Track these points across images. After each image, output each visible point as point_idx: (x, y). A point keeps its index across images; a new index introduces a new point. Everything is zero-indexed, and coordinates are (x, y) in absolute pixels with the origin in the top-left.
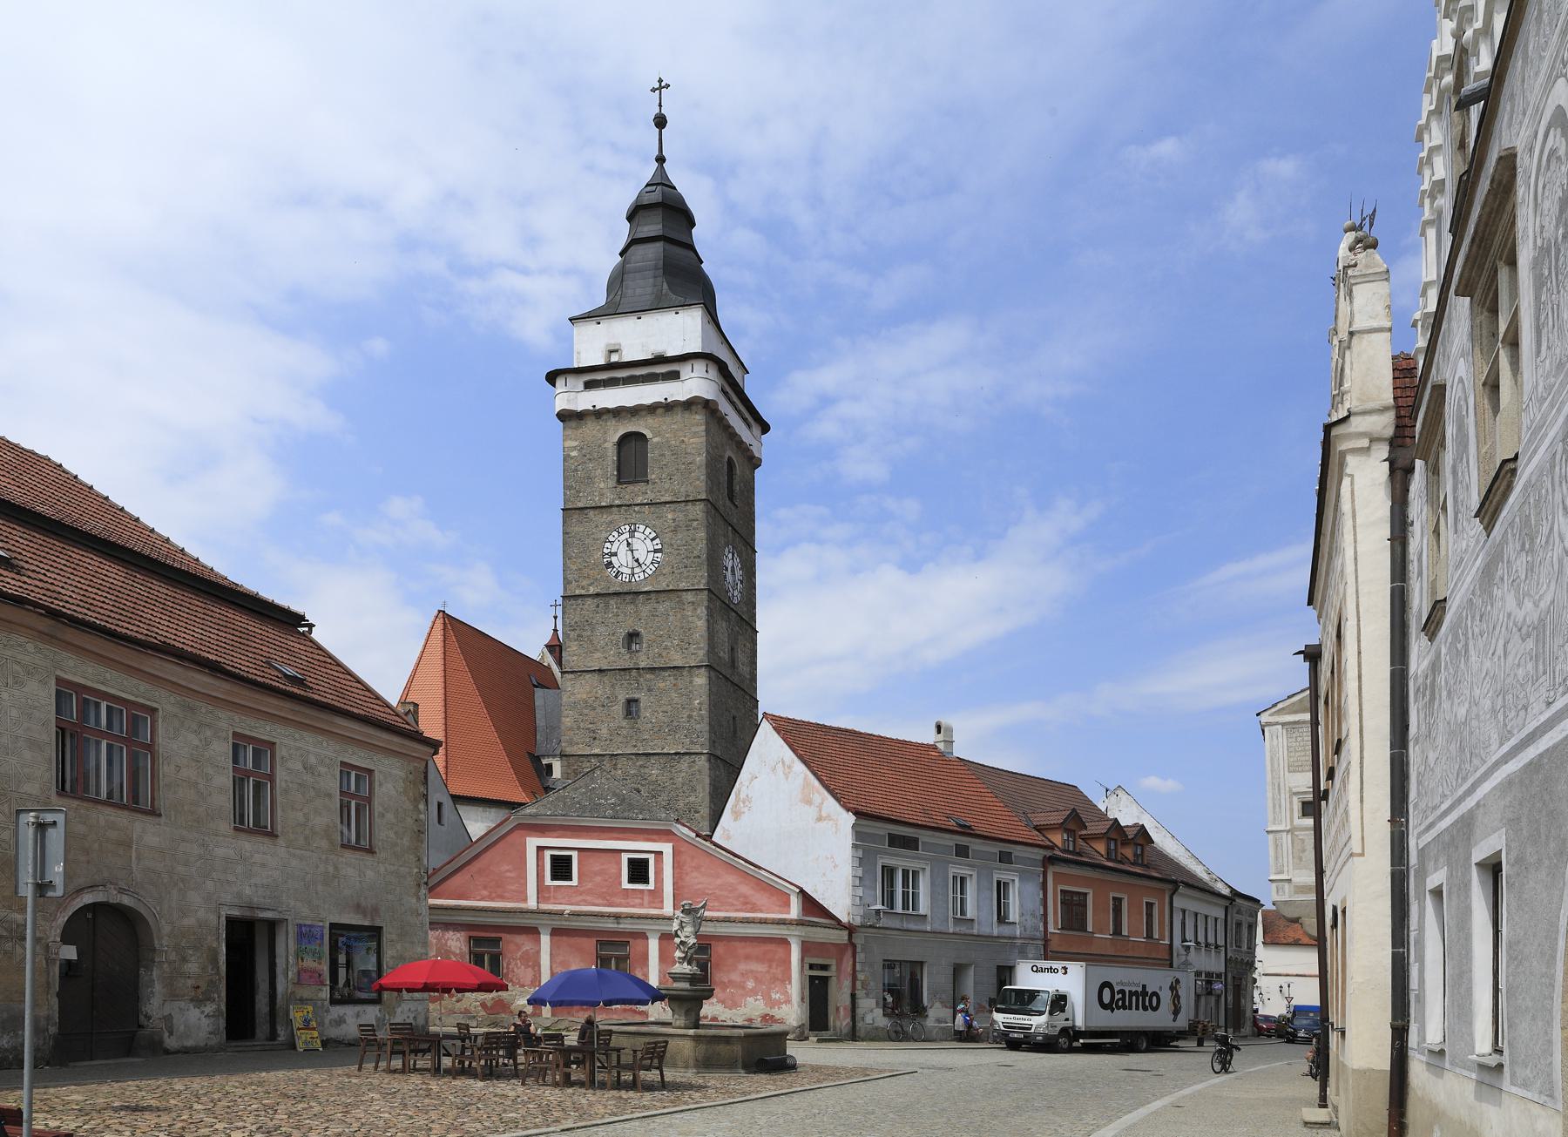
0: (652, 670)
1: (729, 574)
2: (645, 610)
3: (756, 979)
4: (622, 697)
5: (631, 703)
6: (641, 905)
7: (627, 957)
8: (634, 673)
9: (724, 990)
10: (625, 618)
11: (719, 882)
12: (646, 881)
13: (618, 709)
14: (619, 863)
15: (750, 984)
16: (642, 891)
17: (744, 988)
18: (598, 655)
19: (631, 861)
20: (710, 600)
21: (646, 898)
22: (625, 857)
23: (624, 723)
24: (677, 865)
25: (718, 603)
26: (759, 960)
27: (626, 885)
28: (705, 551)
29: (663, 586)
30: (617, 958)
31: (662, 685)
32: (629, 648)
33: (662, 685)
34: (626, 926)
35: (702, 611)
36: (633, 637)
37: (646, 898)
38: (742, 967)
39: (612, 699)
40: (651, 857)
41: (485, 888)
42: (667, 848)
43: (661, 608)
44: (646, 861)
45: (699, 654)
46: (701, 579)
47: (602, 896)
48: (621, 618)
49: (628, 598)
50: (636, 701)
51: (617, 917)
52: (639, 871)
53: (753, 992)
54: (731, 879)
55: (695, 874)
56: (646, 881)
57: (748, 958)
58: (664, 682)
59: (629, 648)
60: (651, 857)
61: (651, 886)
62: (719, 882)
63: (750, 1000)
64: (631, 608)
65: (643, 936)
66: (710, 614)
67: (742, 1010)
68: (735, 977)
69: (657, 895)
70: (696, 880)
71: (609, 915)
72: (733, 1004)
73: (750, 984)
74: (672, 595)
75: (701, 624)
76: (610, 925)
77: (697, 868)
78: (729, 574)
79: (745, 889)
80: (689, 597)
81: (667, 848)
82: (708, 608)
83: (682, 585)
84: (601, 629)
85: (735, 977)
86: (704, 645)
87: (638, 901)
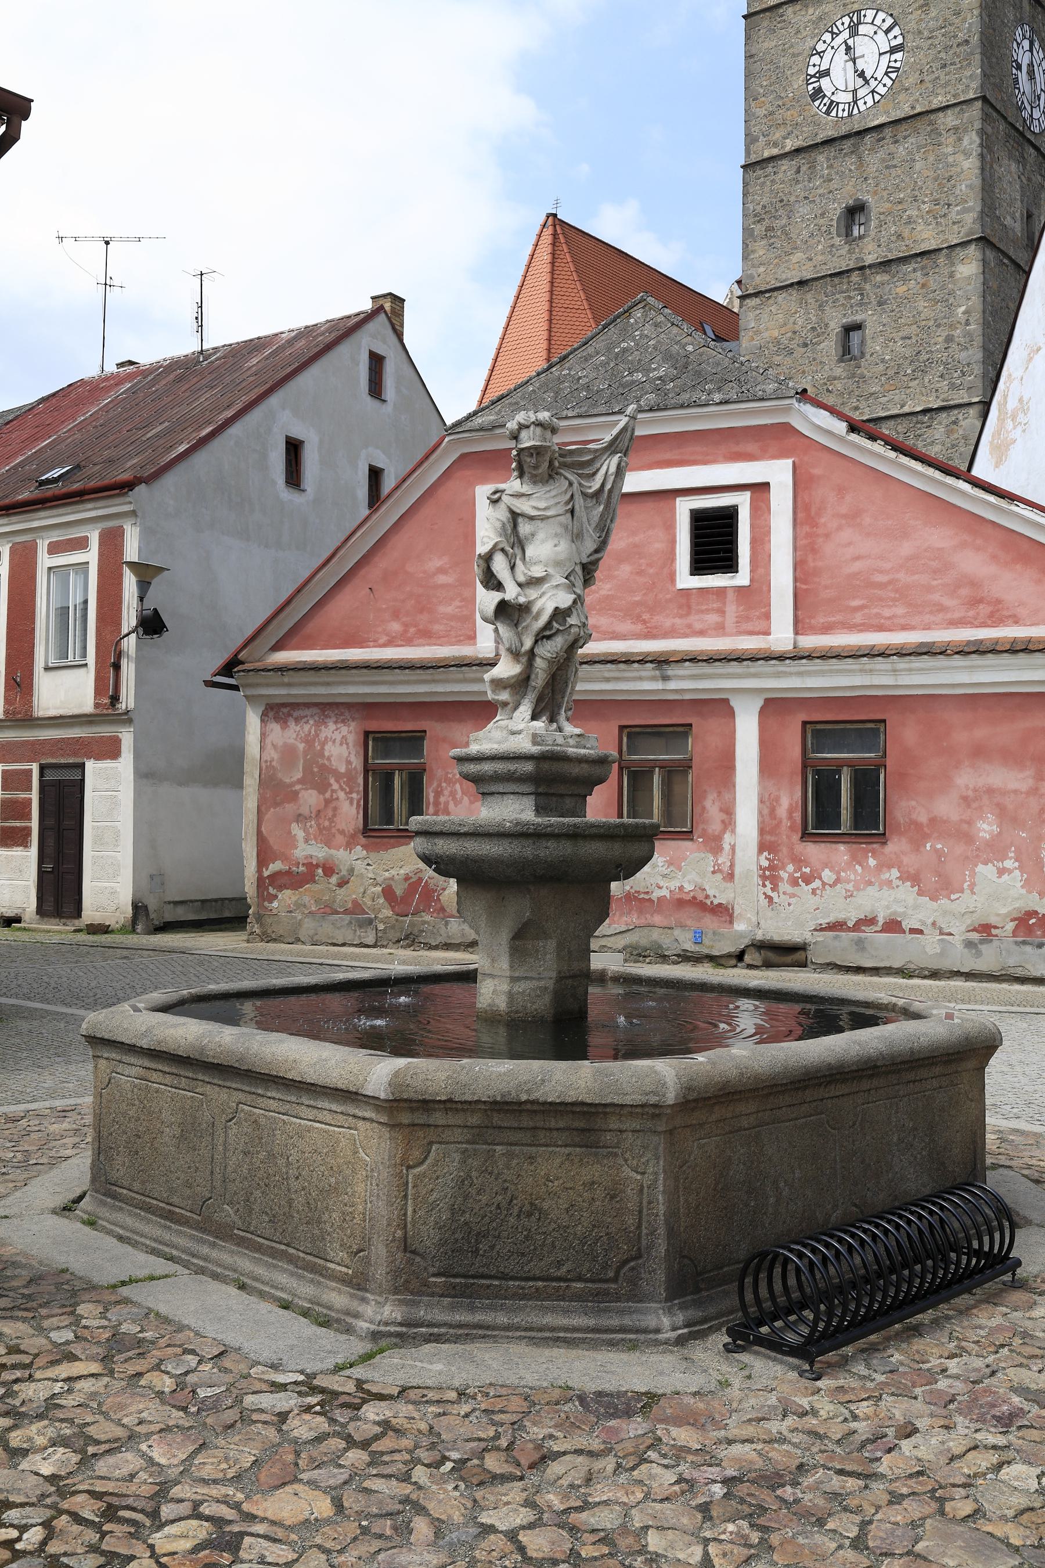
0: (885, 265)
1: (1023, 76)
2: (873, 161)
3: (1002, 812)
4: (836, 321)
5: (849, 329)
6: (720, 630)
7: (685, 766)
8: (855, 277)
9: (917, 846)
10: (840, 182)
11: (907, 548)
12: (729, 564)
13: (830, 346)
14: (670, 526)
15: (986, 828)
16: (721, 592)
17: (967, 837)
18: (799, 256)
19: (700, 519)
20: (986, 118)
21: (732, 609)
22: (684, 508)
23: (838, 371)
24: (804, 514)
25: (1002, 126)
26: (1010, 757)
27: (686, 580)
28: (976, 28)
29: (906, 110)
30: (663, 766)
31: (901, 290)
32: (848, 233)
33: (901, 290)
34: (683, 683)
35: (972, 141)
36: (855, 211)
37: (732, 609)
38: (966, 779)
39: (818, 330)
40: (743, 501)
41: (396, 615)
42: (778, 473)
43: (901, 151)
44: (729, 515)
45: (966, 219)
46: (969, 82)
47: (631, 613)
48: (834, 185)
49: (847, 145)
50: (858, 327)
51: (661, 661)
52: (715, 540)
53: (995, 851)
54: (938, 537)
55: (846, 534)
56: (729, 564)
57: (979, 753)
58: (906, 285)
59: (848, 233)
60: (743, 501)
61: (742, 577)
62: (907, 548)
63: (986, 871)
64: (851, 162)
65: (720, 708)
66: (987, 144)
67: (965, 902)
68: (946, 808)
69: (755, 597)
70: (851, 549)
71: (643, 660)
72: (943, 886)
73: (986, 828)
74: (919, 124)
75: (969, 166)
76: (645, 684)
77: (853, 517)
78: (1023, 76)
79: (974, 563)
80: (949, 119)
81: (778, 473)
82: (982, 132)
83: (937, 101)
84: (803, 209)
85: (946, 808)
86: (974, 203)
87: (713, 618)
